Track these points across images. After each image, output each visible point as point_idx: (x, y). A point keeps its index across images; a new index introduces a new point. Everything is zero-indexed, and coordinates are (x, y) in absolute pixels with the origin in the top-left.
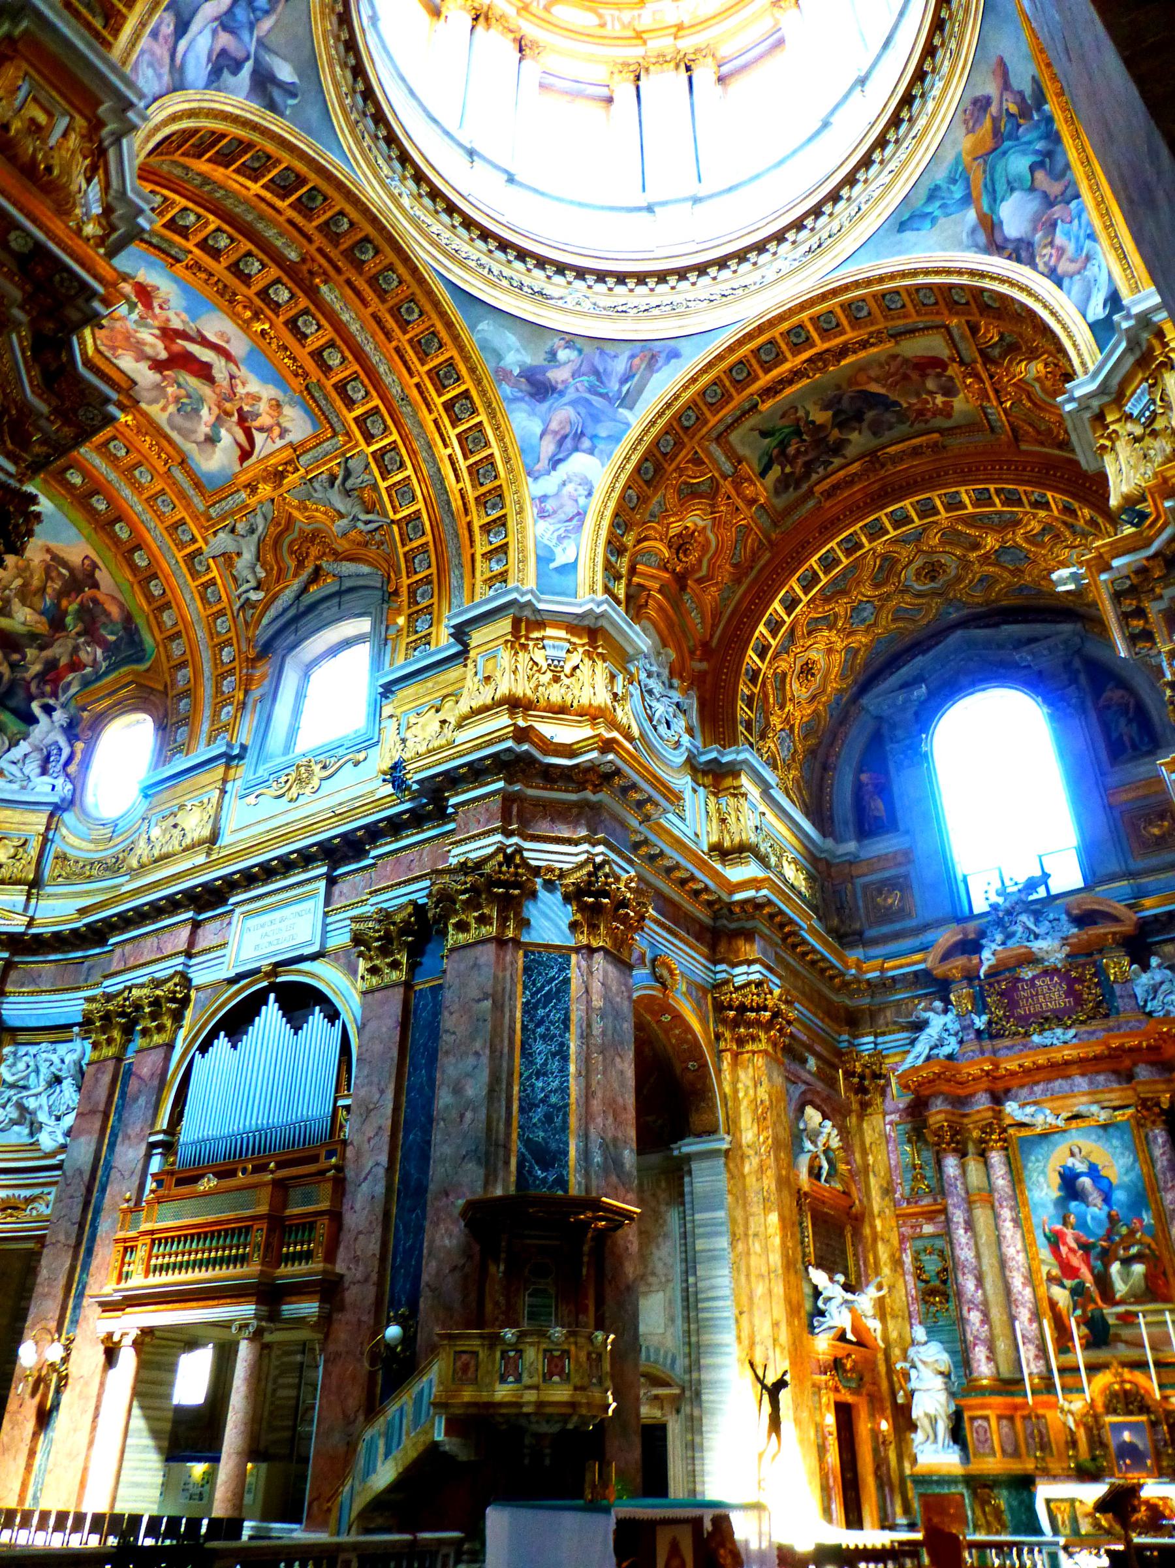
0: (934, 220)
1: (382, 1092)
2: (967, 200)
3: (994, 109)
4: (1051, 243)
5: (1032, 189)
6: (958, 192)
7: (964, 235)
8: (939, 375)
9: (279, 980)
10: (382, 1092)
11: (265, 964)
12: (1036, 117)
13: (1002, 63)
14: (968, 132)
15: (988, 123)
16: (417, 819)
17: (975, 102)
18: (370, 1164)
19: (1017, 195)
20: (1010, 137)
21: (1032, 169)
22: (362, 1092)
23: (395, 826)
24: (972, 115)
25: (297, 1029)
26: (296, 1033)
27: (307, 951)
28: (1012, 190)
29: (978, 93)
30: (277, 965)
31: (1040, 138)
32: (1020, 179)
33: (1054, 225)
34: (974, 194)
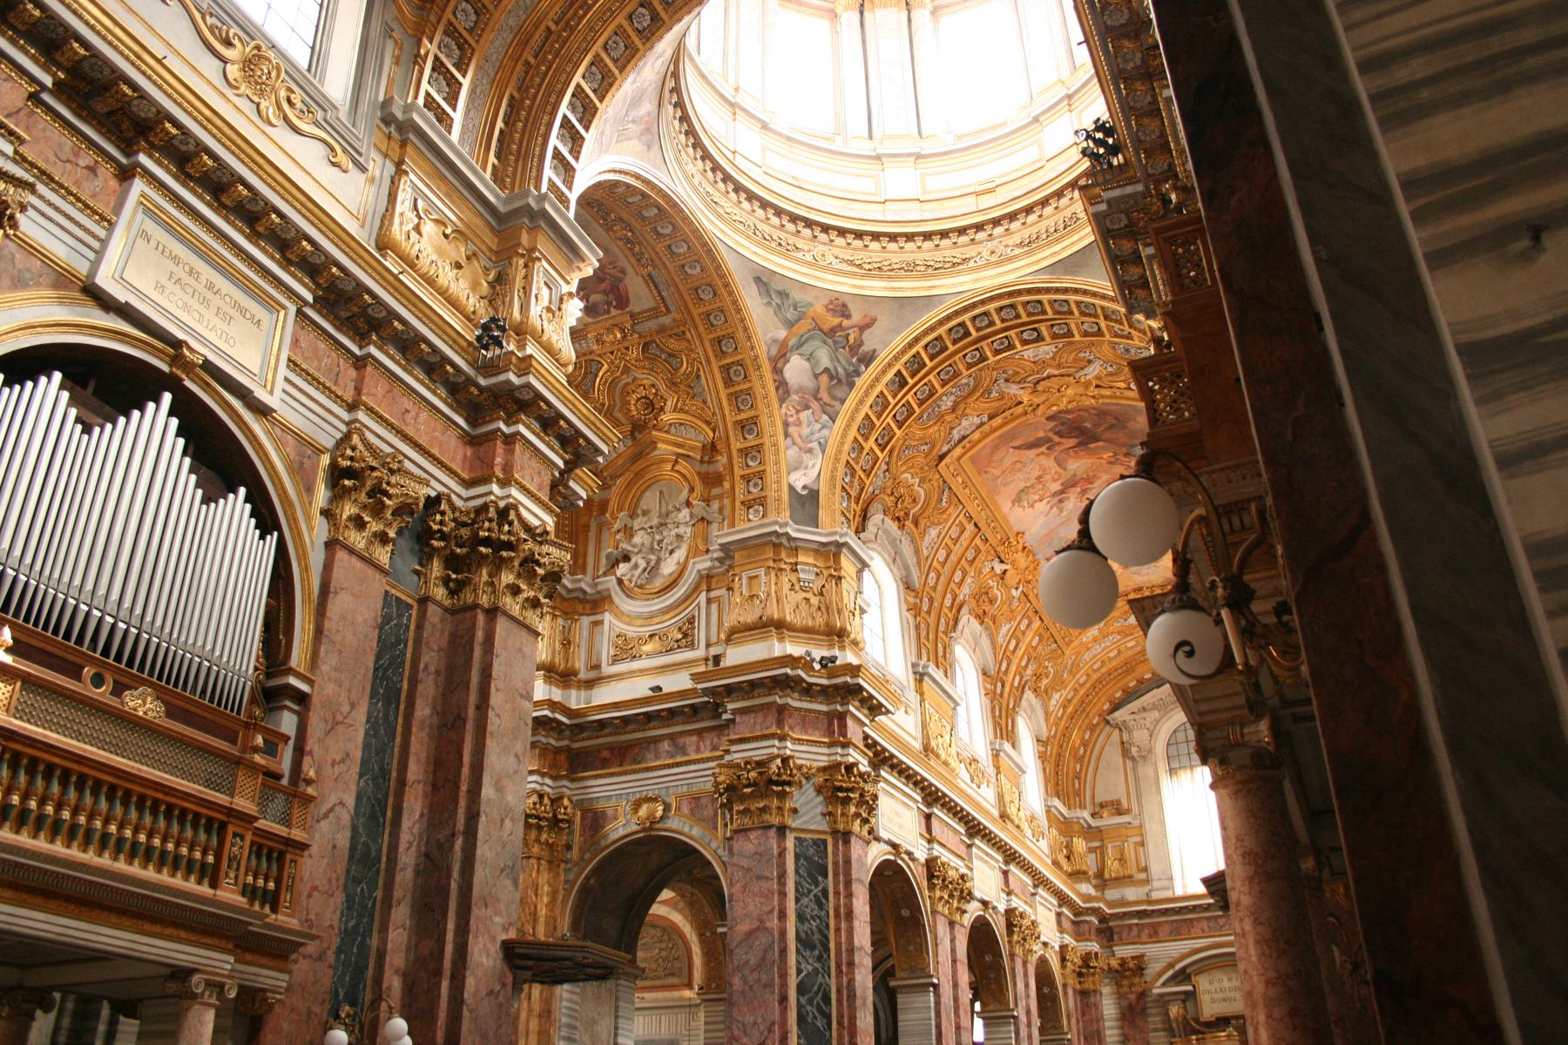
0: (769, 304)
1: (353, 706)
2: (790, 325)
3: (846, 323)
4: (798, 412)
5: (816, 376)
6: (791, 315)
7: (770, 335)
8: (609, 304)
9: (188, 383)
10: (353, 706)
11: (200, 350)
12: (854, 360)
13: (873, 321)
14: (826, 306)
15: (837, 321)
16: (457, 389)
17: (844, 305)
18: (333, 799)
19: (807, 364)
20: (835, 343)
21: (826, 370)
22: (330, 688)
23: (434, 367)
24: (837, 305)
25: (206, 500)
26: (206, 500)
27: (261, 394)
28: (808, 359)
29: (850, 306)
30: (208, 366)
31: (845, 370)
32: (817, 363)
33: (807, 407)
34: (794, 329)
